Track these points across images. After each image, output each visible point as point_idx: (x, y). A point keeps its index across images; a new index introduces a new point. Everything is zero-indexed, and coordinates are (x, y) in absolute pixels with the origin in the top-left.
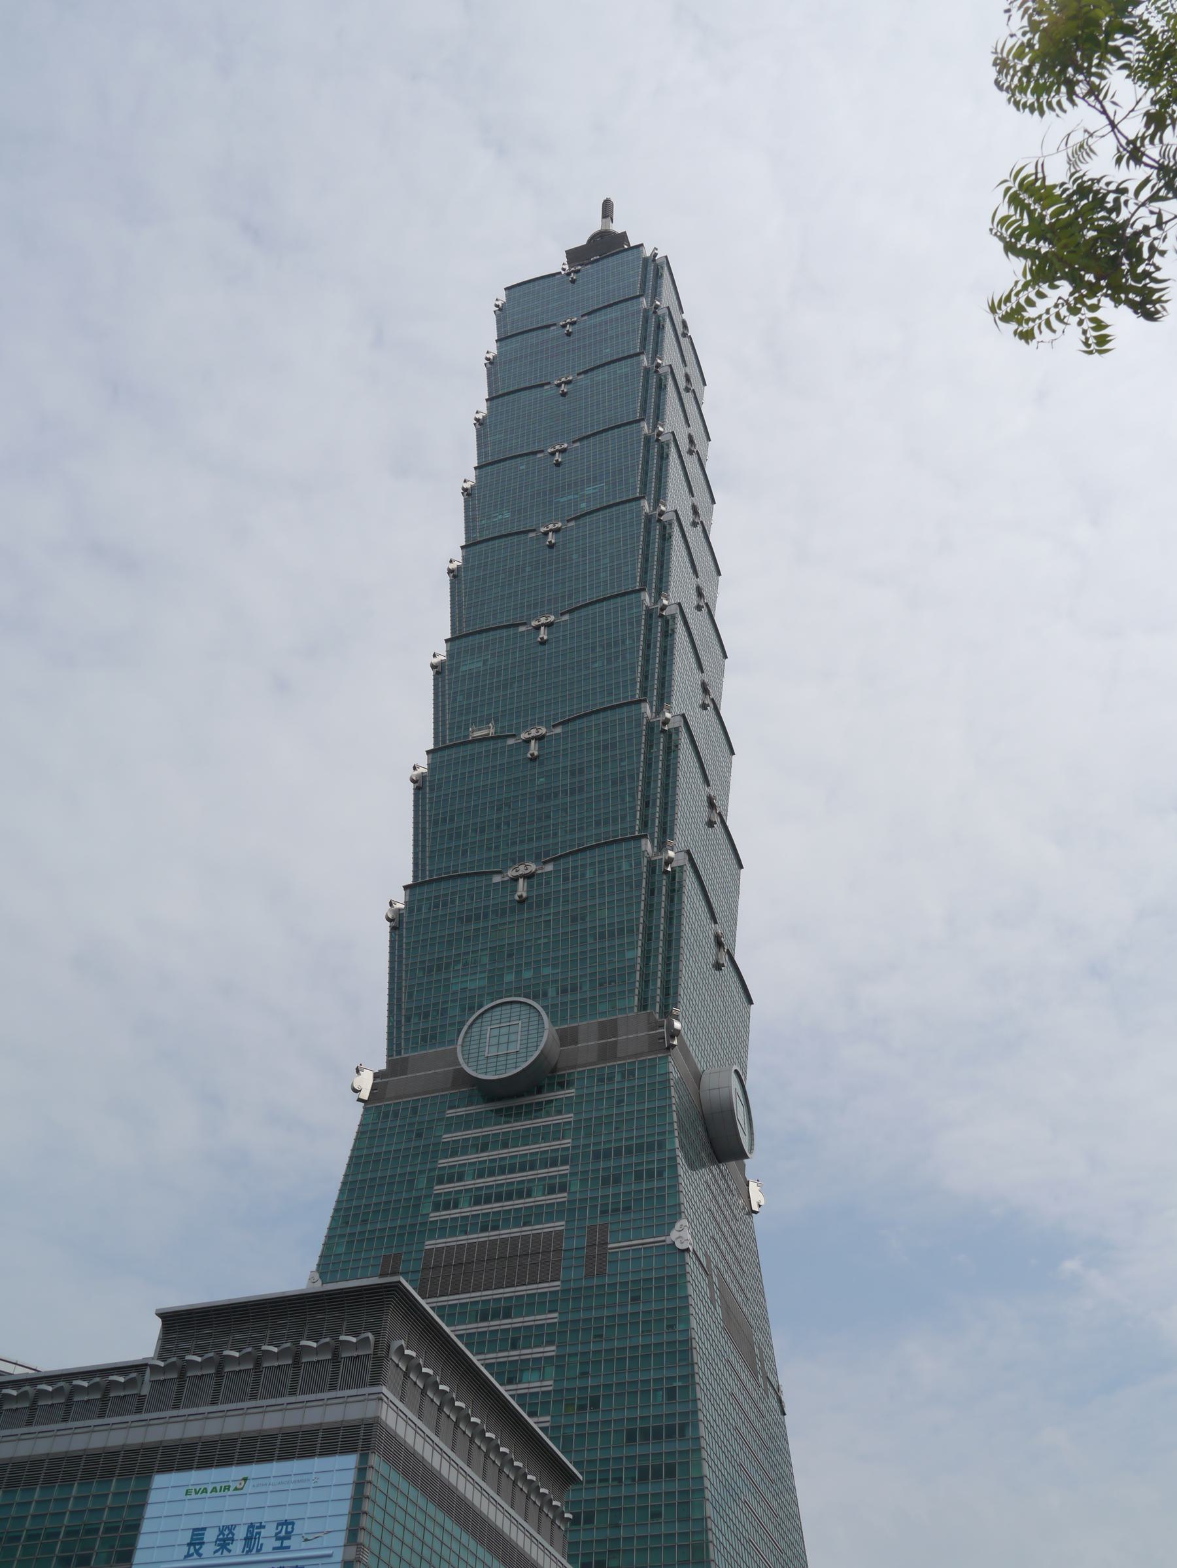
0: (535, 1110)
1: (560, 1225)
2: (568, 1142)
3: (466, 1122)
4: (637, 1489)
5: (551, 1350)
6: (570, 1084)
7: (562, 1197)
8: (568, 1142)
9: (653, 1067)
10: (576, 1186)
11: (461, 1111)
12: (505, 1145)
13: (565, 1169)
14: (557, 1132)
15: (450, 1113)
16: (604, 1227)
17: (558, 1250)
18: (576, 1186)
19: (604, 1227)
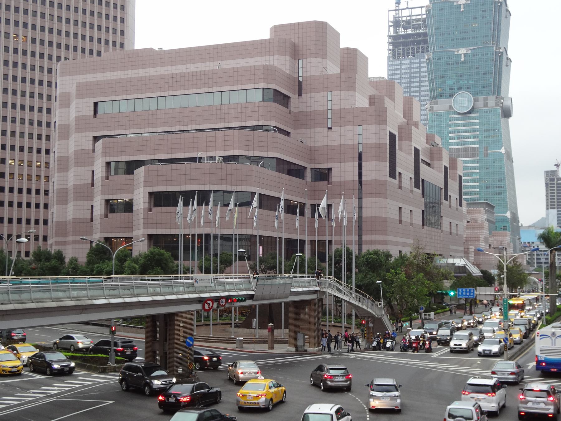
0: (469, 119)
1: (478, 146)
2: (478, 127)
3: (454, 119)
4: (495, 196)
5: (478, 171)
6: (477, 112)
7: (478, 139)
8: (478, 127)
9: (496, 111)
10: (480, 137)
11: (453, 116)
12: (464, 126)
13: (478, 133)
14: (475, 124)
15: (450, 116)
16: (487, 147)
17: (478, 151)
18: (480, 137)
19: (487, 147)
